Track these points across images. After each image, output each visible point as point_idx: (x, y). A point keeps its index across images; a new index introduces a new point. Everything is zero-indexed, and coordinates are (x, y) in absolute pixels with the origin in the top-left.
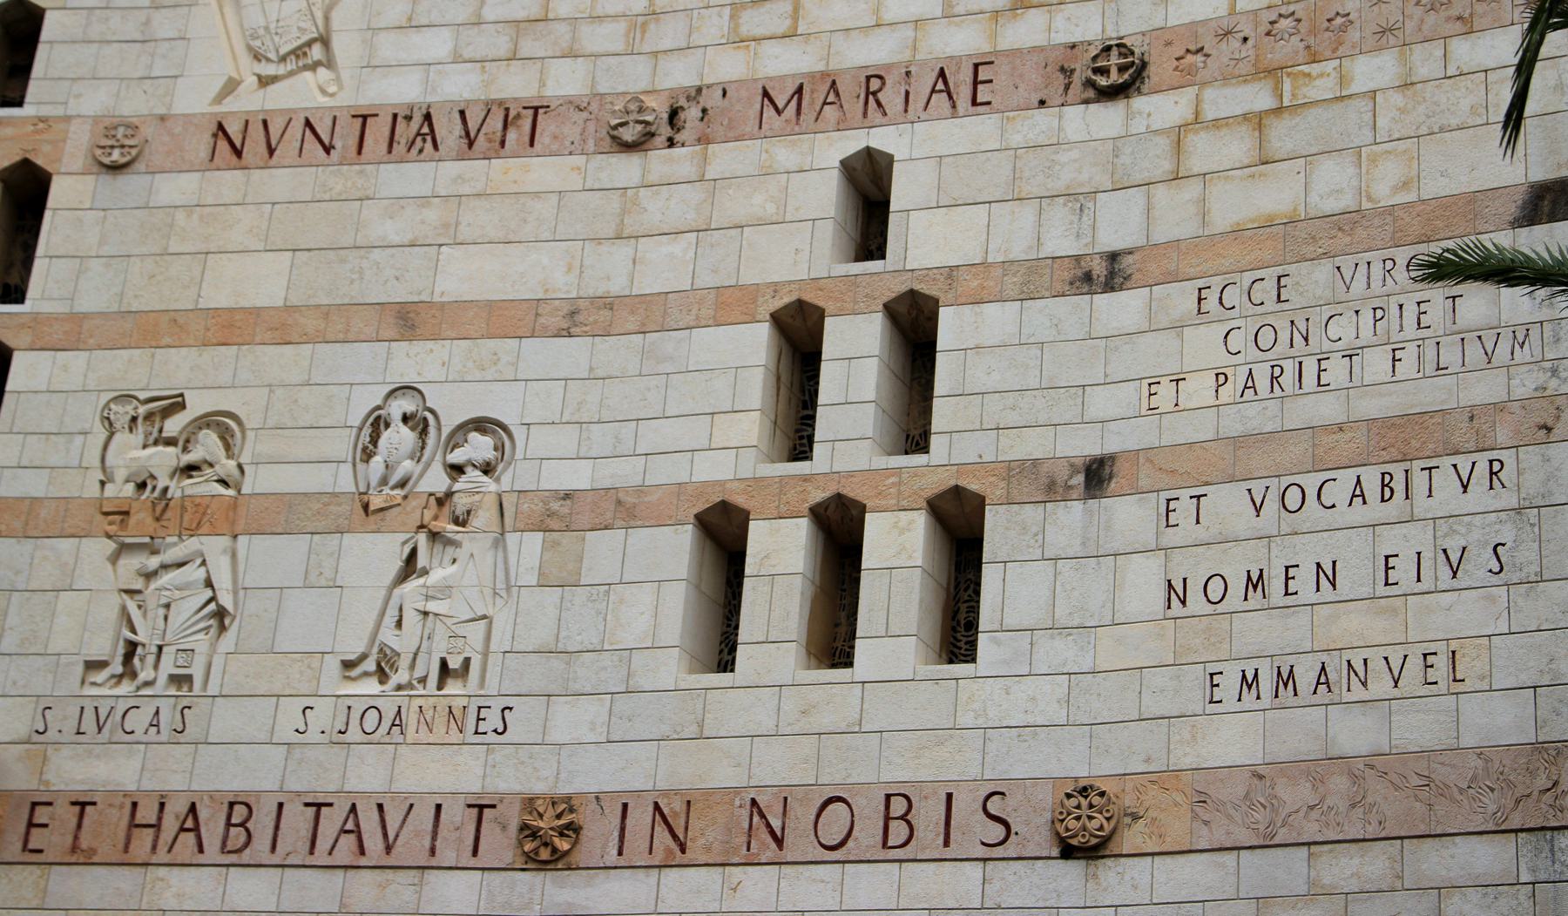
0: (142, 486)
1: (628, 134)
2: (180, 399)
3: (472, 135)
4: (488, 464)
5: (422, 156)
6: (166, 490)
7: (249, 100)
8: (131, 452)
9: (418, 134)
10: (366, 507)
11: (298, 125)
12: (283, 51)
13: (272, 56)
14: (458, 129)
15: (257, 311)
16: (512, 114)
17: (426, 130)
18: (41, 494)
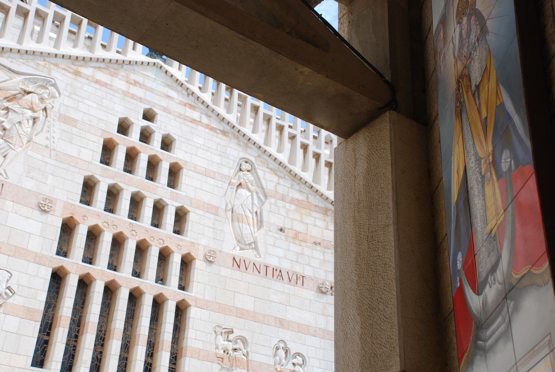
0: (224, 351)
1: (324, 290)
2: (232, 330)
3: (290, 279)
4: (301, 365)
5: (280, 281)
6: (230, 354)
7: (237, 252)
8: (222, 342)
9: (279, 275)
10: (276, 369)
11: (252, 264)
12: (247, 243)
13: (243, 243)
14: (287, 277)
15: (248, 311)
16: (298, 276)
17: (280, 274)
18: (201, 348)
